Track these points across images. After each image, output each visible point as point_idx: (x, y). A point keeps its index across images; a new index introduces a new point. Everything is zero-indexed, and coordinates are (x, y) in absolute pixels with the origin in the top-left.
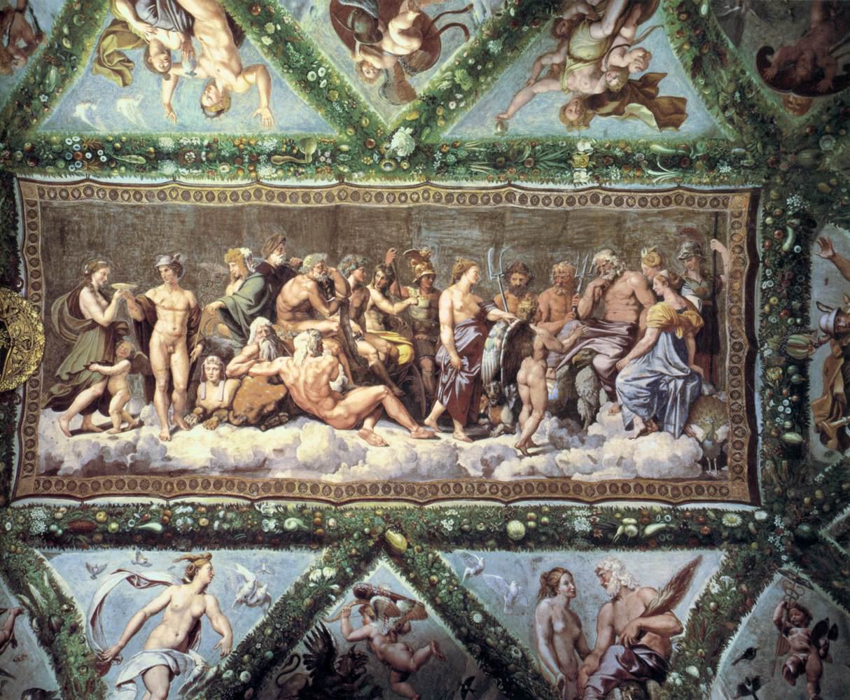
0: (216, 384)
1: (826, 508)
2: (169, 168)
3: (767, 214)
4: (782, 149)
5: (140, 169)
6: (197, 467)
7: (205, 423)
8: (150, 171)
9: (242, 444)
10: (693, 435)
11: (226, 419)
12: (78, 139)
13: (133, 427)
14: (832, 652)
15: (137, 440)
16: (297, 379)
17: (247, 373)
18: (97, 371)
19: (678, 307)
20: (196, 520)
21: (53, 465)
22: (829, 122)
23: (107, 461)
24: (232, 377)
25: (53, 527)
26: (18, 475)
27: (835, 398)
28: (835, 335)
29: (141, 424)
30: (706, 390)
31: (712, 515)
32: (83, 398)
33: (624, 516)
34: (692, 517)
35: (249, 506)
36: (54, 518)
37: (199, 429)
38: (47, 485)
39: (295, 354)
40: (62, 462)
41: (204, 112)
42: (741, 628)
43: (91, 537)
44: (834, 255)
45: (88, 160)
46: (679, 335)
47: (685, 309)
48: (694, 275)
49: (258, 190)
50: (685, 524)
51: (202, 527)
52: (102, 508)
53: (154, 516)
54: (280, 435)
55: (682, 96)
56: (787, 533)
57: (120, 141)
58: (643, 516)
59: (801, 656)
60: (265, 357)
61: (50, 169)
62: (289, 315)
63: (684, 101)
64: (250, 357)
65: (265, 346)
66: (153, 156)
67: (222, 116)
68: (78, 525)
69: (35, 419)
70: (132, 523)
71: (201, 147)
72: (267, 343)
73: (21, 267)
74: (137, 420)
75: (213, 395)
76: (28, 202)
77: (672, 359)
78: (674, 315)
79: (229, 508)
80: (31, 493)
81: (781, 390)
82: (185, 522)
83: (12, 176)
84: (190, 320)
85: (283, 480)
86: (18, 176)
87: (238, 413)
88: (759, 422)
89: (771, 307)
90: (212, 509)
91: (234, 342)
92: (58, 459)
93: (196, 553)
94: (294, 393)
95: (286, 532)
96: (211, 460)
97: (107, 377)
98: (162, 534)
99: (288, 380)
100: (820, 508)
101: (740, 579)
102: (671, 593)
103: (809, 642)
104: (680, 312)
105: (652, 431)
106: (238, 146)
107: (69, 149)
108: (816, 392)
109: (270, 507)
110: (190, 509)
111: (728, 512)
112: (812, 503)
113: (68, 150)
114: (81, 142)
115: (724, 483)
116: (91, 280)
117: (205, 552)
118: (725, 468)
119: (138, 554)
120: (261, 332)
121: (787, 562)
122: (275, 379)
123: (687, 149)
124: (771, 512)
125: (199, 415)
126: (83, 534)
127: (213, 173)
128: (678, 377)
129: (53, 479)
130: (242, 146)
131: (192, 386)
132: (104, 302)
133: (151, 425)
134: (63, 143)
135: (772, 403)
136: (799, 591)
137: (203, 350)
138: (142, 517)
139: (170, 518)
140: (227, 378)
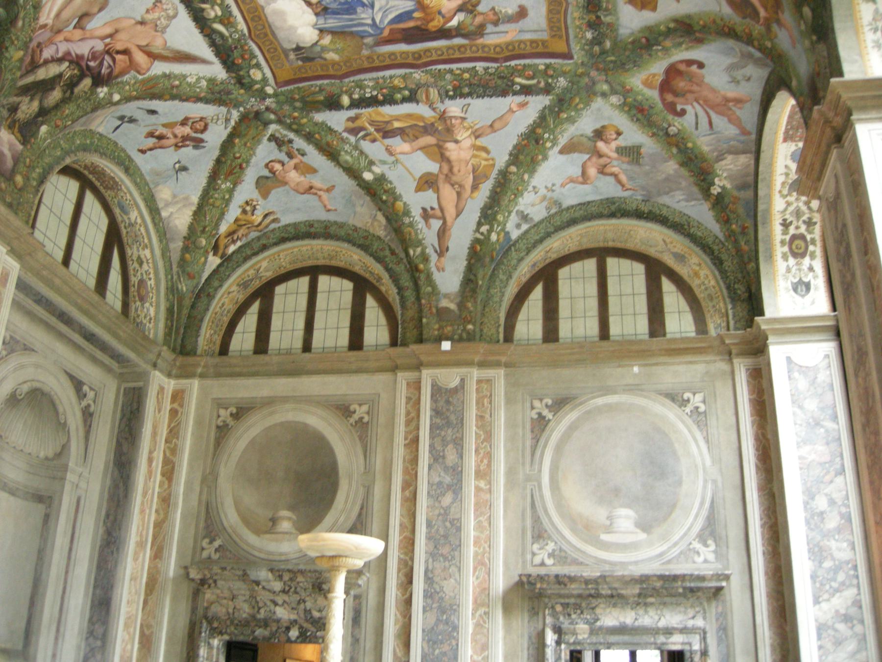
1: (295, 127)
3: (548, 66)
4: (610, 73)
10: (321, 38)
14: (183, 149)
19: (444, 11)
22: (635, 100)
27: (387, 122)
28: (443, 117)
30: (369, 40)
31: (254, 62)
33: (221, 5)
34: (246, 51)
42: (169, 103)
44: (514, 112)
46: (416, 15)
47: (443, 17)
48: (478, 20)
50: (236, 48)
55: (658, 9)
56: (263, 107)
58: (228, 19)
59: (170, 135)
63: (654, 9)
77: (391, 12)
78: (435, 9)
81: (386, 88)
88: (352, 79)
89: (458, 75)
100: (292, 124)
101: (210, 90)
102: (170, 55)
103: (182, 137)
104: (440, 13)
105: (313, 10)
108: (388, 110)
111: (262, 71)
112: (295, 118)
115: (287, 65)
118: (300, 63)
121: (238, 111)
123: (607, 10)
124: (275, 95)
128: (373, 20)
135: (371, 84)
136: (219, 122)
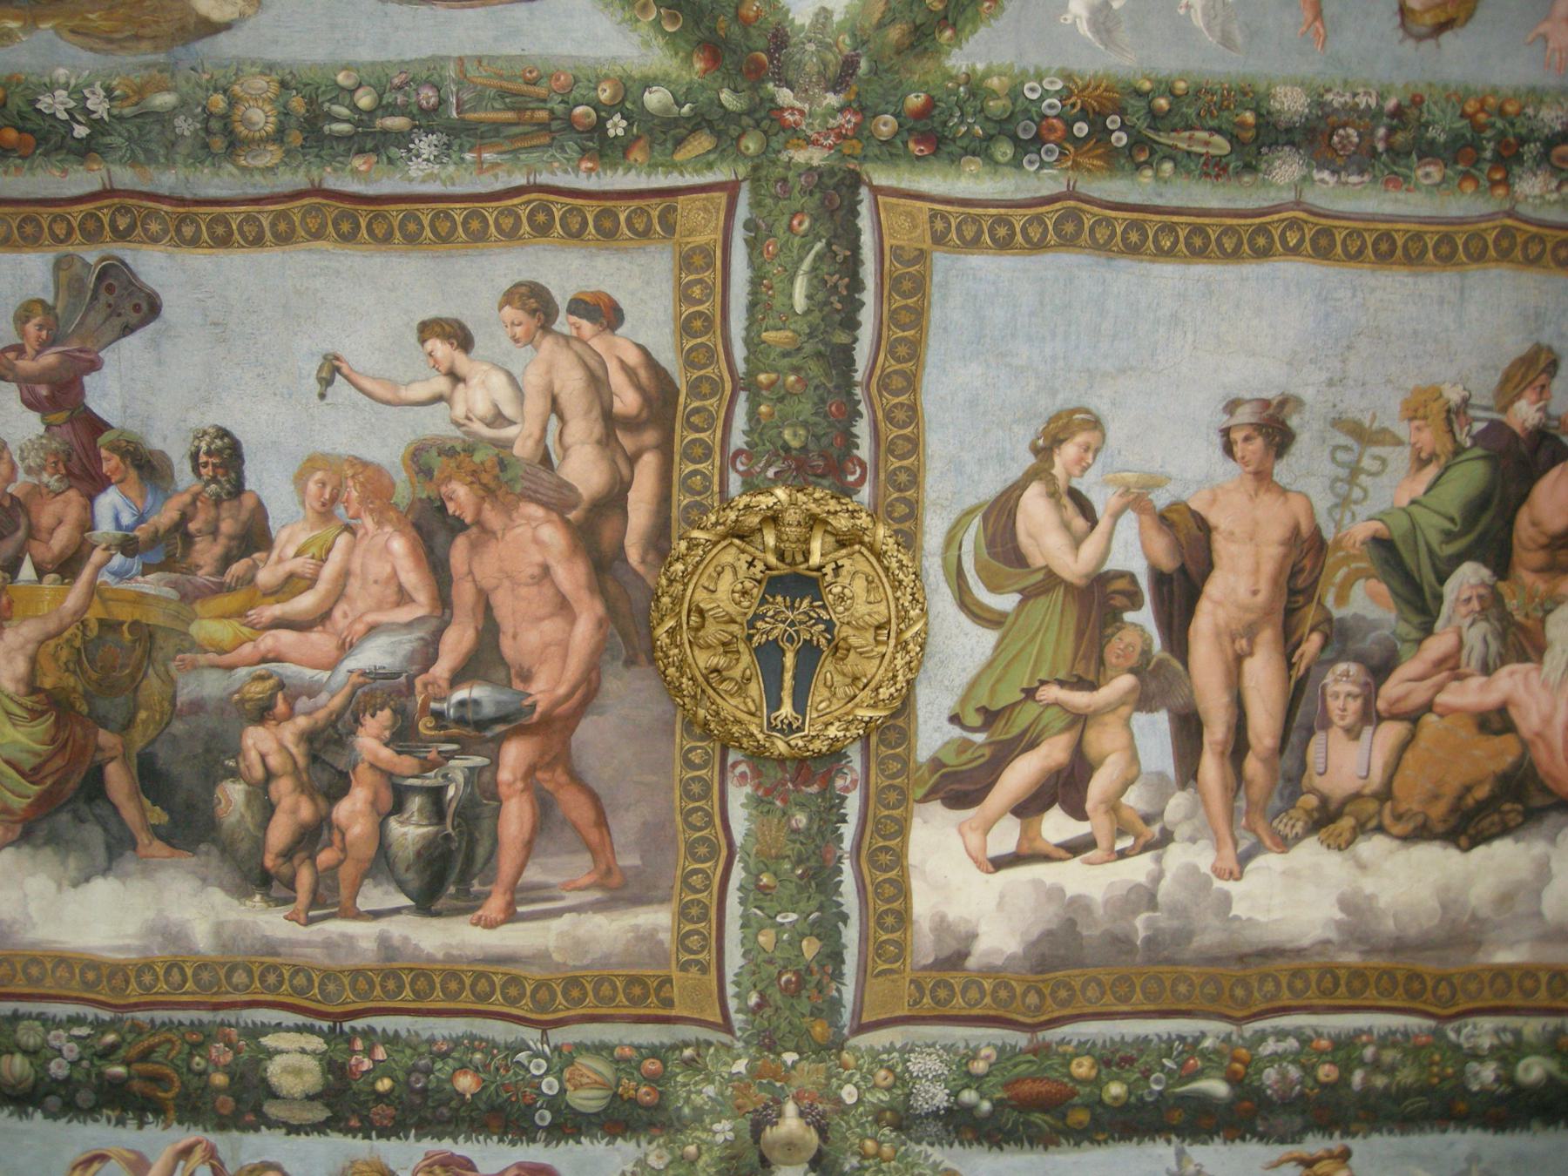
0: (1353, 733)
2: (1286, 169)
5: (1215, 169)
6: (1306, 942)
7: (1323, 833)
8: (1238, 174)
9: (1408, 880)
11: (1373, 823)
12: (1059, 86)
13: (1146, 848)
15: (1157, 878)
16: (1547, 721)
17: (1429, 707)
18: (1056, 703)
20: (1309, 1070)
21: (951, 946)
23: (1085, 933)
24: (1394, 717)
25: (969, 1096)
26: (863, 969)
29: (1166, 838)
32: (1021, 774)
35: (1437, 1034)
36: (968, 1073)
37: (1310, 852)
38: (942, 994)
39: (1548, 657)
40: (973, 936)
41: (1403, 25)
43: (1064, 1116)
45: (1076, 141)
49: (1505, 232)
51: (1324, 1086)
52: (1085, 1048)
53: (1214, 1061)
54: (1503, 859)
57: (1170, 92)
60: (1475, 663)
61: (973, 165)
62: (1538, 558)
64: (1439, 664)
65: (1477, 636)
66: (1251, 134)
67: (1447, 37)
68: (1026, 1088)
69: (902, 830)
70: (1158, 1081)
71: (1375, 115)
72: (1482, 627)
73: (862, 429)
74: (1155, 829)
75: (1347, 761)
76: (897, 252)
79: (1387, 1040)
80: (905, 1012)
82: (1284, 1076)
83: (855, 181)
84: (1294, 575)
85: (1512, 967)
86: (881, 178)
87: (1403, 807)
90: (1345, 1048)
91: (1403, 628)
92: (962, 928)
93: (1314, 1145)
94: (1541, 755)
95: (1519, 1090)
96: (1339, 924)
97: (1080, 721)
98: (1230, 1106)
99: (1529, 720)
106: (1471, 117)
107: (1029, 111)
109: (1483, 1031)
110: (1292, 1043)
113: (1026, 111)
114: (1065, 95)
116: (1052, 465)
117: (1336, 1143)
119: (1180, 1155)
120: (1469, 600)
122: (1497, 721)
125: (1308, 813)
126: (1045, 1111)
127: (1398, 181)
129: (956, 979)
130: (1482, 117)
131: (1294, 739)
132: (1079, 523)
133: (1193, 840)
134: (1015, 93)
137: (1323, 648)
138: (1182, 1065)
139: (1247, 1065)
140: (1380, 719)
